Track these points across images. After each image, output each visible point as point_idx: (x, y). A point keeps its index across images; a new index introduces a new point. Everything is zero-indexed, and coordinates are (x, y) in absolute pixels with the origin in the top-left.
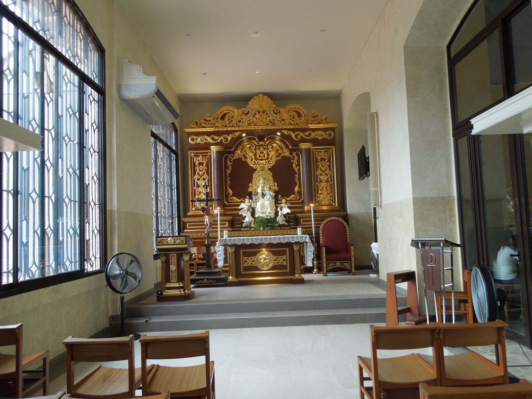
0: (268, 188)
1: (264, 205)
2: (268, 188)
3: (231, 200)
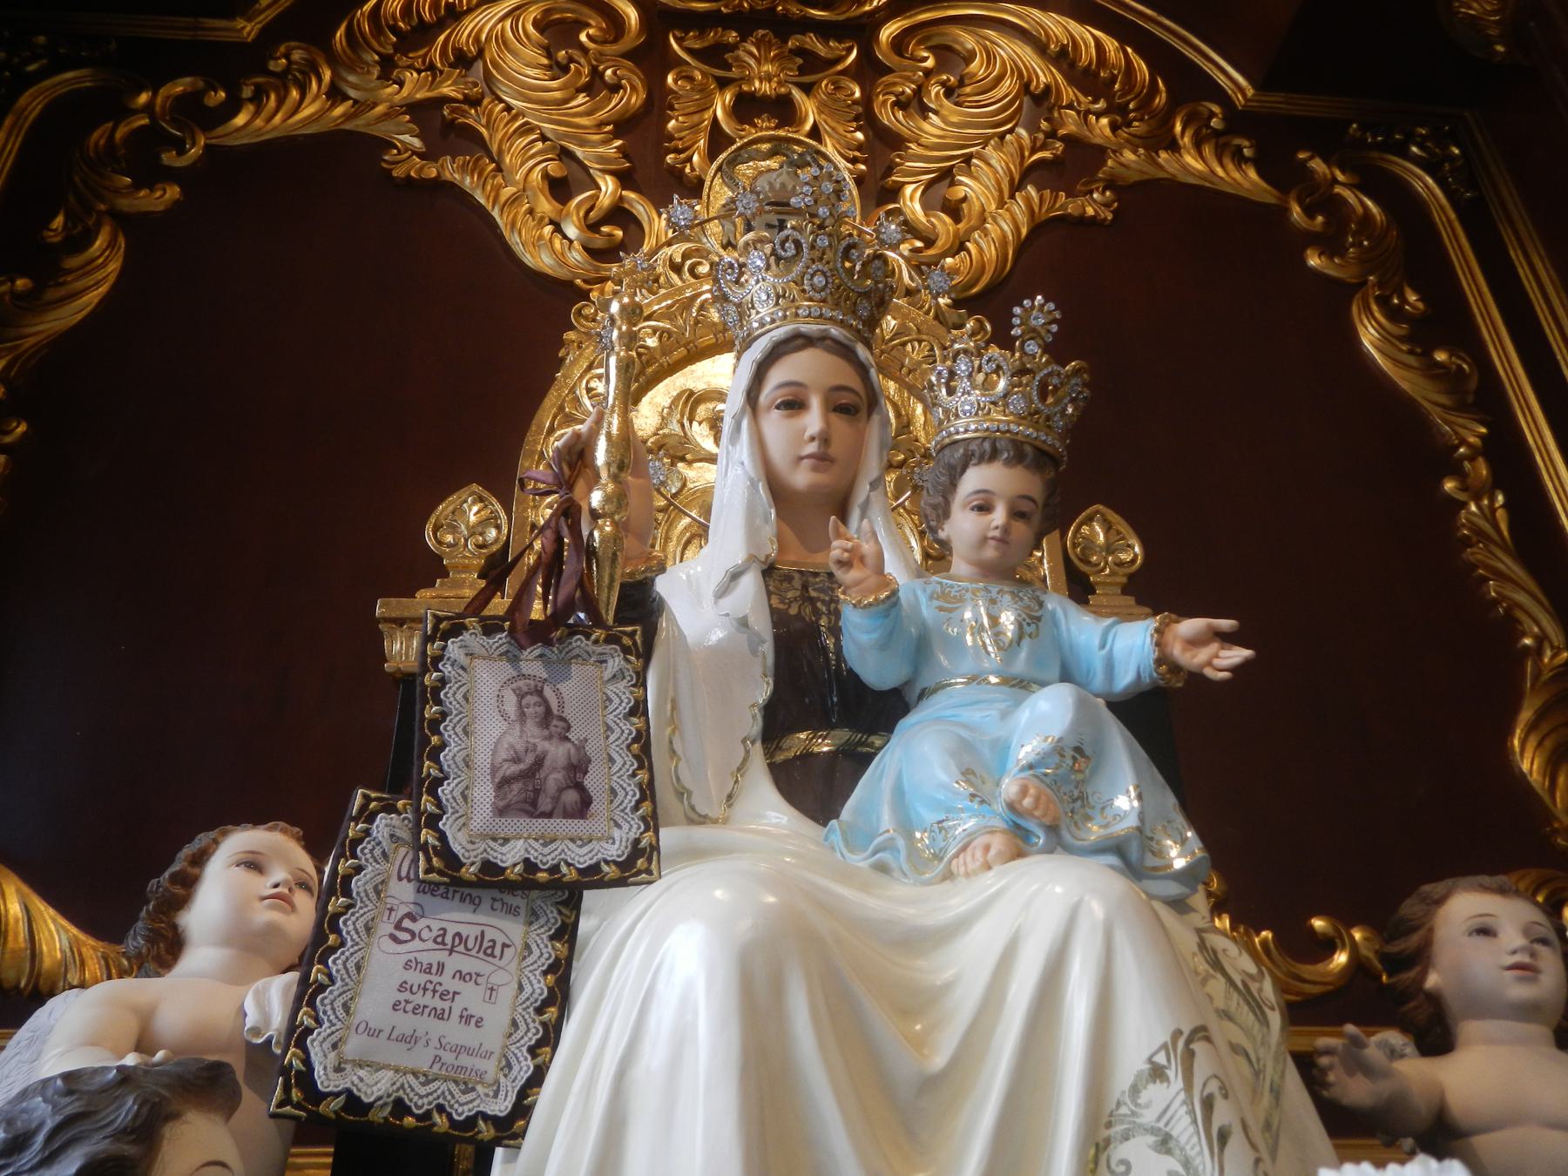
0: (974, 479)
2: (989, 450)
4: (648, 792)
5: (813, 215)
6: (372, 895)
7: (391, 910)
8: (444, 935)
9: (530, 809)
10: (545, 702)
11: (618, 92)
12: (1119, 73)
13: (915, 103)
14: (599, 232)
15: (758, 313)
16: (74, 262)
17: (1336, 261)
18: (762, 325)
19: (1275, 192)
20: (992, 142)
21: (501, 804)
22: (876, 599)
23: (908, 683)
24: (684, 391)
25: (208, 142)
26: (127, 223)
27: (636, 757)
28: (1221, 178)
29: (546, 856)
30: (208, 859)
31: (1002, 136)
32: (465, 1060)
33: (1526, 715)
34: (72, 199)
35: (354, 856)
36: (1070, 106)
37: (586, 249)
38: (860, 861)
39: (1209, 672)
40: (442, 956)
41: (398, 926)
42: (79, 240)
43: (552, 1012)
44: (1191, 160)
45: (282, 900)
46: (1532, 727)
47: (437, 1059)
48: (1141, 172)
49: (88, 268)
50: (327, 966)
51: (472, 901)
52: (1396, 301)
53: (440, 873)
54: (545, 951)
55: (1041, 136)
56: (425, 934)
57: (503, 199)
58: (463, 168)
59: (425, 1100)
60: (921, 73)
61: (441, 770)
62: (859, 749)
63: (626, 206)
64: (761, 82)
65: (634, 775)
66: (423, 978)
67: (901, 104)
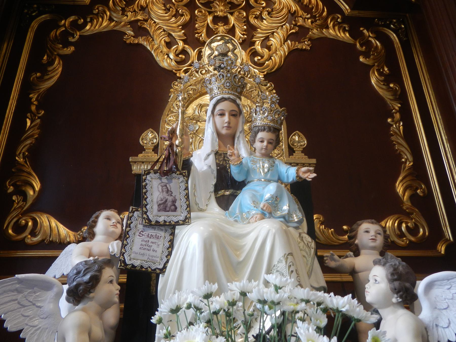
0: (260, 135)
1: (238, 248)
3: (19, 229)
4: (188, 206)
5: (227, 69)
6: (135, 227)
7: (138, 230)
8: (149, 235)
9: (164, 210)
10: (167, 188)
11: (183, 16)
12: (314, 6)
13: (260, 17)
14: (178, 57)
15: (214, 92)
16: (50, 68)
17: (367, 59)
18: (215, 95)
19: (353, 40)
20: (280, 28)
21: (159, 209)
22: (237, 164)
23: (246, 180)
24: (199, 104)
25: (80, 34)
26: (62, 57)
27: (186, 199)
28: (339, 37)
29: (168, 219)
30: (99, 217)
31: (282, 26)
32: (154, 258)
33: (400, 178)
34: (48, 51)
35: (131, 220)
36: (301, 17)
37: (175, 61)
38: (232, 220)
39: (307, 179)
40: (149, 239)
41: (140, 233)
42: (51, 63)
43: (170, 249)
44: (331, 31)
45: (115, 226)
46: (401, 181)
47: (148, 258)
48: (318, 35)
49: (54, 70)
50: (127, 241)
51: (154, 228)
52: (381, 70)
53: (148, 223)
54: (168, 238)
55: (292, 26)
56: (145, 235)
57: (154, 48)
58: (144, 40)
59: (147, 266)
60: (262, 8)
61: (147, 203)
62: (235, 194)
63: (185, 49)
64: (220, 12)
65: (186, 202)
66: (145, 243)
67: (256, 18)
